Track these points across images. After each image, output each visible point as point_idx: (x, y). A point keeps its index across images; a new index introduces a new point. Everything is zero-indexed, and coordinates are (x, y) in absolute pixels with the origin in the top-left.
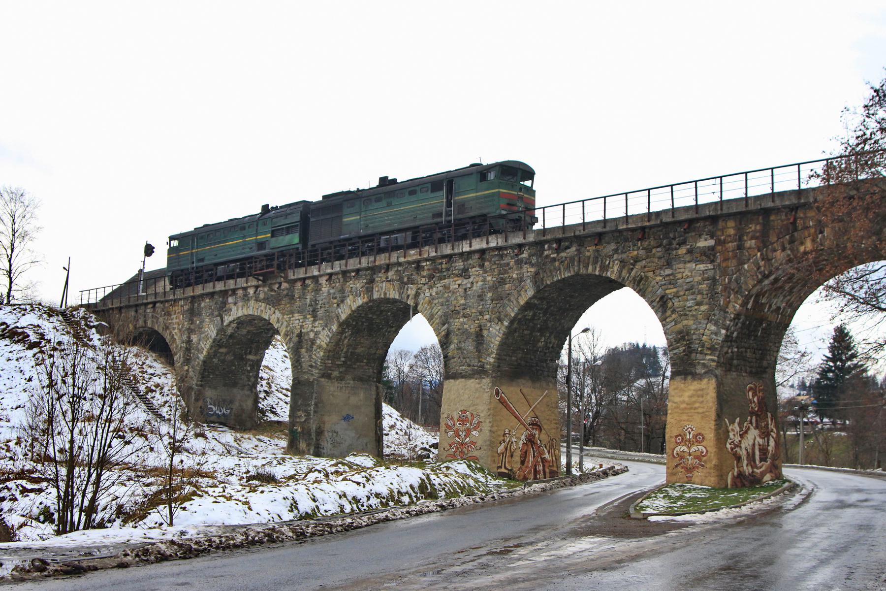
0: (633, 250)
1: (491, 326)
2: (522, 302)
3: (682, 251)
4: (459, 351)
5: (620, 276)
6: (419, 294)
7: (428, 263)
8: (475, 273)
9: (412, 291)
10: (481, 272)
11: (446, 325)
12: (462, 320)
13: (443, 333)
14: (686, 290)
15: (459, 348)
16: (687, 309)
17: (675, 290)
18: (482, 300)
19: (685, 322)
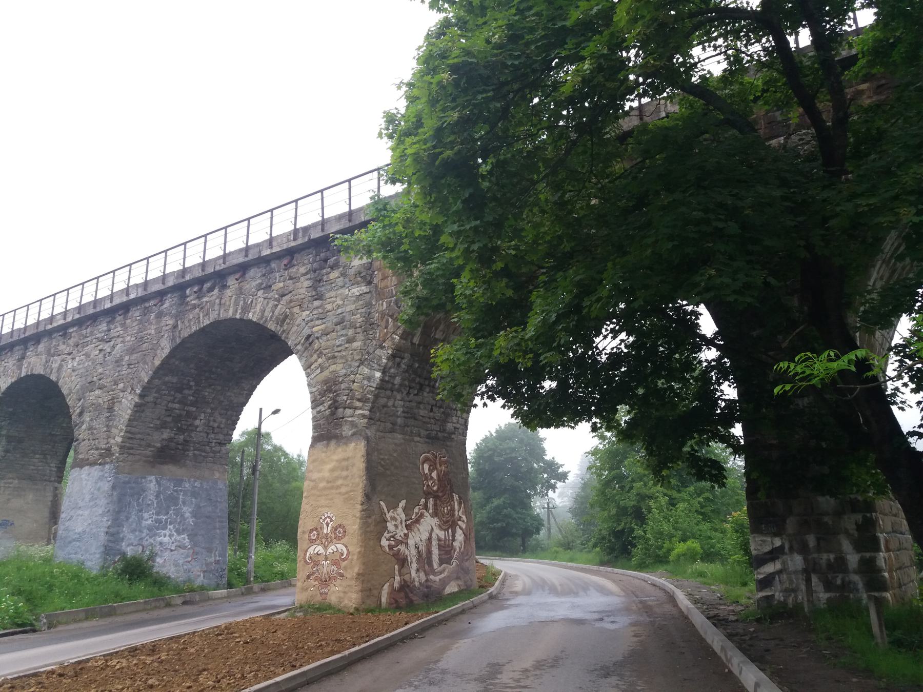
0: (279, 282)
2: (157, 362)
3: (335, 274)
7: (75, 329)
9: (55, 366)
11: (82, 400)
15: (90, 428)
16: (336, 349)
17: (323, 326)
18: (118, 366)
19: (333, 367)
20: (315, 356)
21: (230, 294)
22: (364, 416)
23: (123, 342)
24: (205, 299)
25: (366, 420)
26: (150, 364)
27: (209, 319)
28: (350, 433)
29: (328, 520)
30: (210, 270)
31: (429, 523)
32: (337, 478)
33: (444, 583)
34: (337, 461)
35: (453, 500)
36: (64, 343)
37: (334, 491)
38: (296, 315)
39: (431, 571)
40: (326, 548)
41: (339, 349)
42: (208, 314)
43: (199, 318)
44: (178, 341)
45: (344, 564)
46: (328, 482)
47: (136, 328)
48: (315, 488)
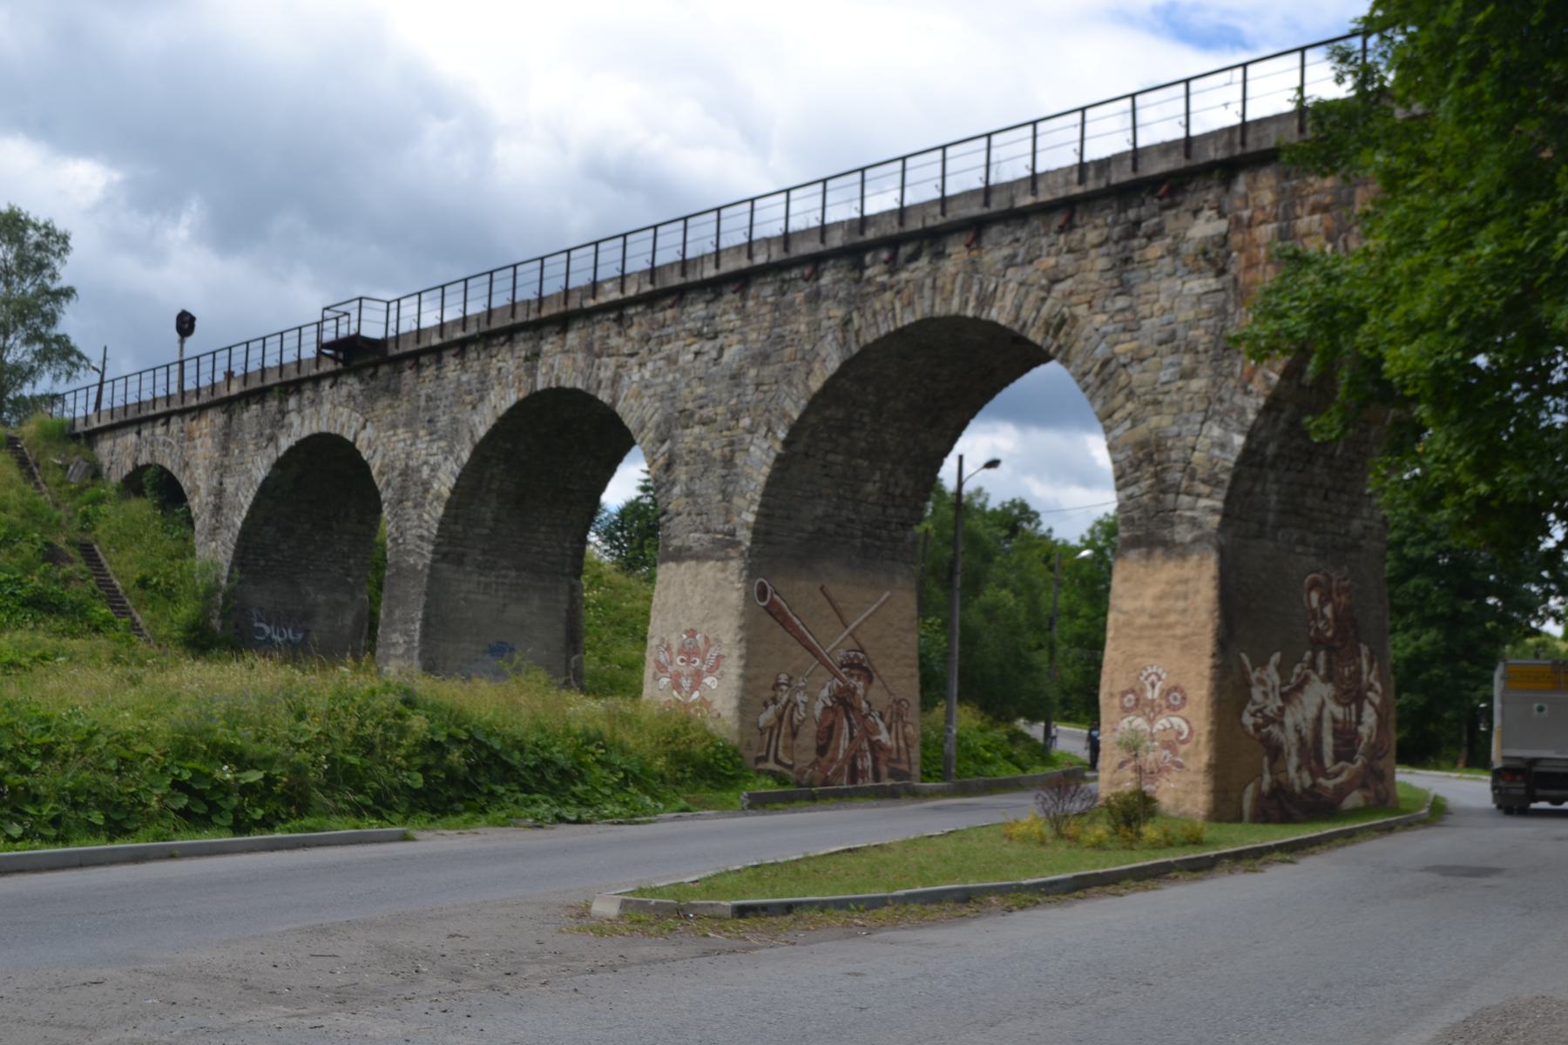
0: (1049, 254)
1: (751, 443)
2: (816, 384)
3: (1156, 249)
4: (690, 500)
5: (1017, 319)
6: (621, 377)
8: (726, 326)
9: (606, 374)
10: (738, 323)
12: (697, 430)
13: (661, 461)
14: (1161, 343)
15: (690, 494)
16: (1160, 389)
17: (1134, 344)
18: (737, 385)
19: (1154, 421)
20: (1120, 398)
21: (952, 270)
22: (1214, 510)
23: (743, 341)
24: (904, 275)
25: (1217, 519)
26: (801, 387)
27: (914, 312)
28: (1189, 538)
29: (1153, 677)
30: (914, 224)
31: (1318, 693)
32: (1168, 611)
33: (1342, 792)
34: (1168, 583)
35: (1359, 655)
36: (619, 334)
37: (1163, 632)
38: (1082, 321)
39: (1319, 770)
40: (1151, 721)
41: (1166, 388)
42: (910, 303)
43: (893, 309)
44: (855, 349)
45: (1183, 749)
46: (1152, 616)
47: (768, 317)
48: (1128, 624)
